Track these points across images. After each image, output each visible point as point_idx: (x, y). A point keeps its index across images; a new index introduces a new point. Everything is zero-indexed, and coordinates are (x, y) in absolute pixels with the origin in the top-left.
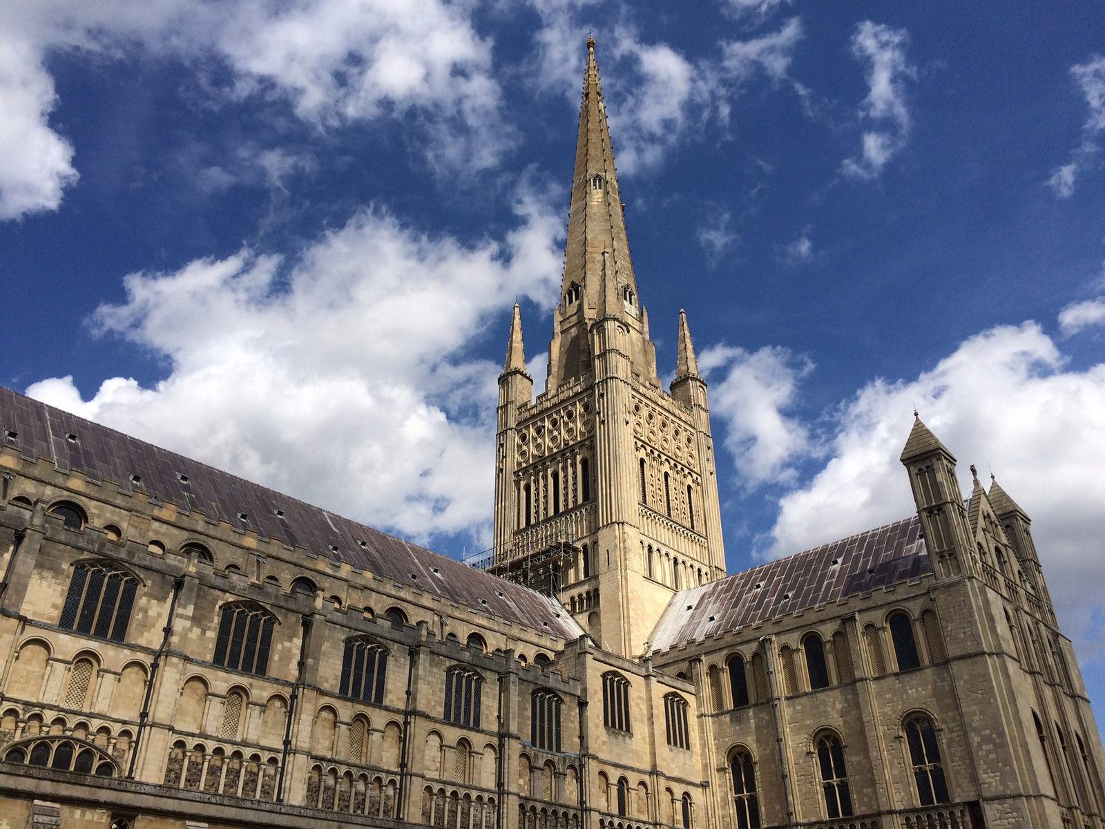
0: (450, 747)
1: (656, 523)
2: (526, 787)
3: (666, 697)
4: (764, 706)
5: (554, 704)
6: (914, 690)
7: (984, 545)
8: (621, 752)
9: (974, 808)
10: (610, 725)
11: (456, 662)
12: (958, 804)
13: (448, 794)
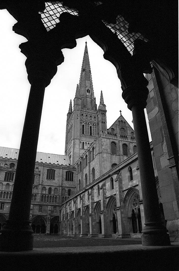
3: (66, 172)
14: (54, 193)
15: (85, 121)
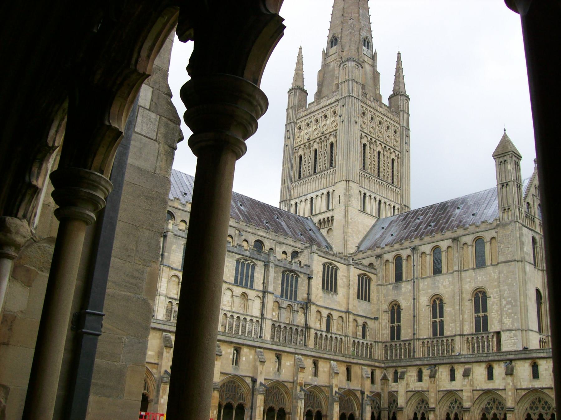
0: (237, 296)
1: (370, 181)
2: (276, 316)
3: (359, 276)
4: (410, 282)
5: (294, 278)
6: (481, 277)
7: (531, 203)
8: (330, 302)
9: (498, 333)
10: (325, 288)
11: (242, 256)
12: (491, 333)
13: (235, 317)
14: (337, 330)
15: (369, 134)
